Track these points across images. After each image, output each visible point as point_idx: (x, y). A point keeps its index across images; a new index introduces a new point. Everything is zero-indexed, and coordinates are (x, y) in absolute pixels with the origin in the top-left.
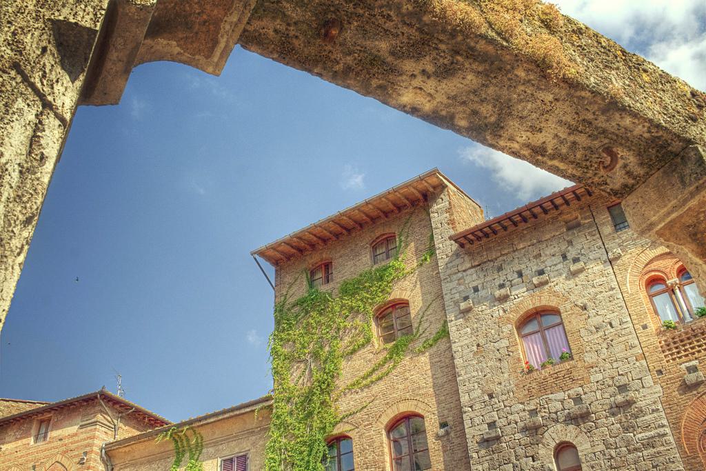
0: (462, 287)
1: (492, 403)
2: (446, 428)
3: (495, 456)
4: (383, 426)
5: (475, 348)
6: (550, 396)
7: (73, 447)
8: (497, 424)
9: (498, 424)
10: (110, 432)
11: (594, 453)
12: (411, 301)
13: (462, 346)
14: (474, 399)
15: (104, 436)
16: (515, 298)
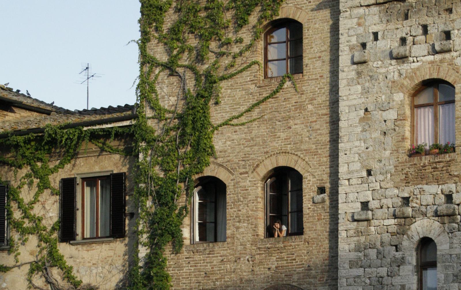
0: (361, 30)
1: (369, 181)
2: (322, 195)
4: (259, 178)
5: (362, 112)
6: (425, 187)
8: (370, 204)
9: (373, 204)
11: (451, 255)
12: (305, 26)
13: (349, 106)
16: (414, 62)
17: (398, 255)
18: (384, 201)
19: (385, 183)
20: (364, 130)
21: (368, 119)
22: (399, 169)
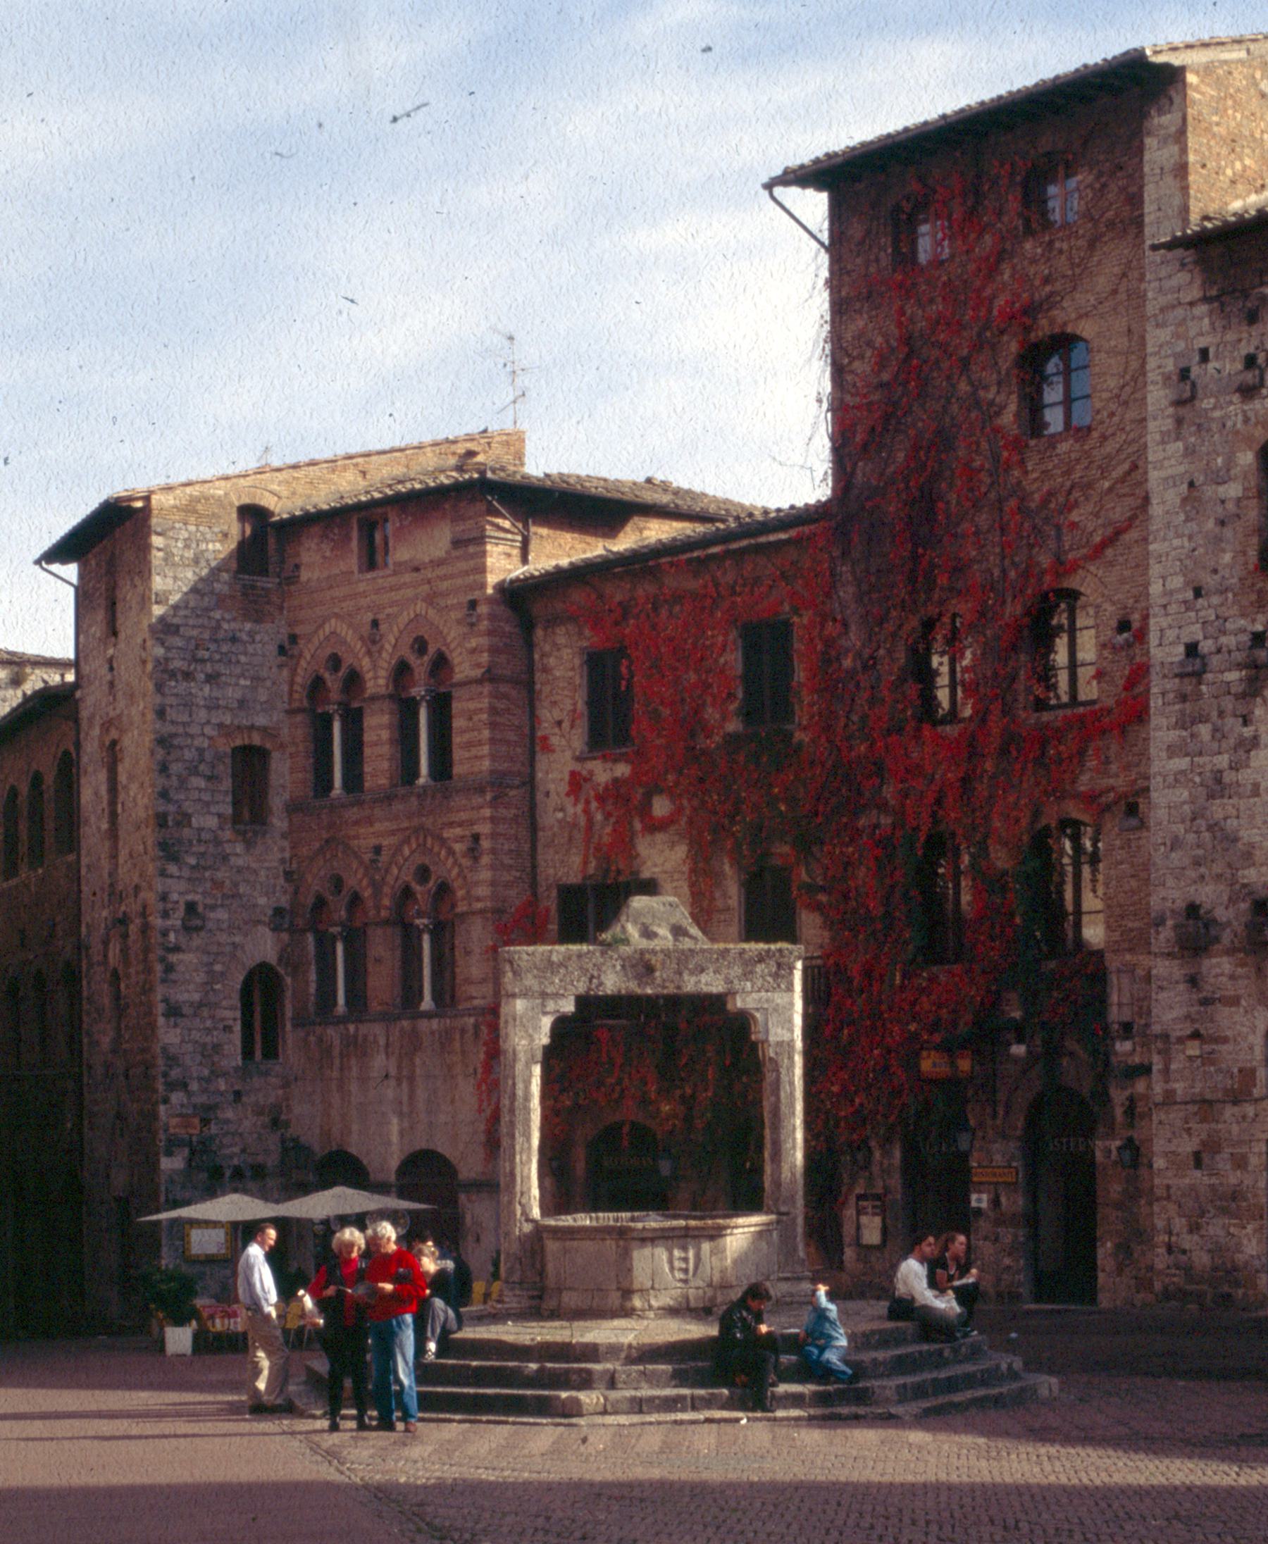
1: (1198, 607)
3: (1188, 705)
7: (445, 585)
9: (1206, 646)
14: (1171, 593)
15: (504, 563)
17: (1248, 732)
18: (1224, 640)
19: (1224, 609)
20: (1187, 520)
21: (1198, 499)
22: (1248, 582)
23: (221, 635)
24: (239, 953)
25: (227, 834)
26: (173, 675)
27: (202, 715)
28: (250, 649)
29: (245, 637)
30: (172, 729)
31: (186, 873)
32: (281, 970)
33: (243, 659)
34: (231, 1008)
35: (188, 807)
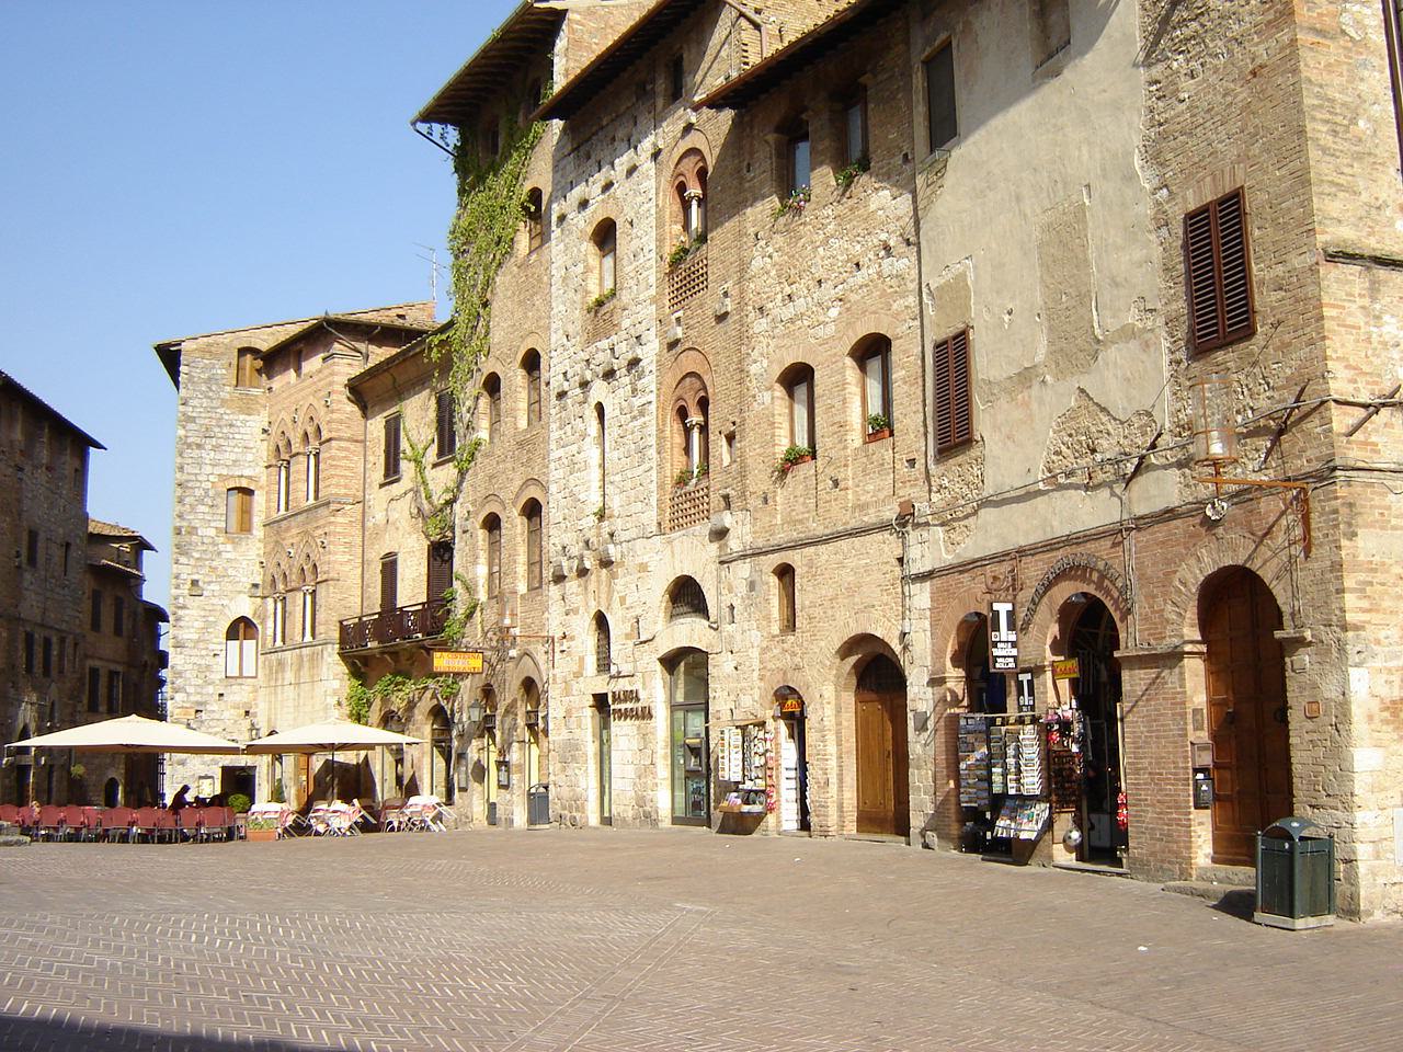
10: (357, 363)
23: (222, 423)
24: (226, 611)
25: (221, 540)
26: (189, 446)
27: (209, 469)
28: (242, 431)
29: (239, 424)
30: (185, 477)
31: (192, 562)
32: (255, 621)
33: (237, 436)
34: (220, 643)
35: (196, 523)
